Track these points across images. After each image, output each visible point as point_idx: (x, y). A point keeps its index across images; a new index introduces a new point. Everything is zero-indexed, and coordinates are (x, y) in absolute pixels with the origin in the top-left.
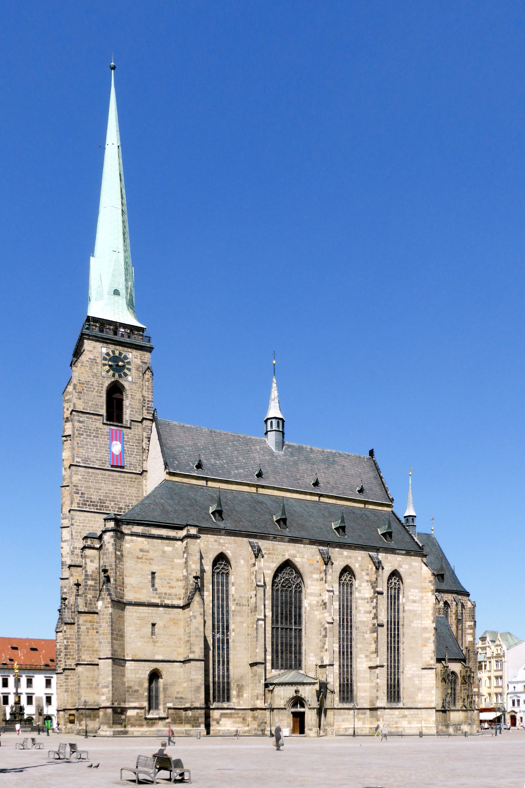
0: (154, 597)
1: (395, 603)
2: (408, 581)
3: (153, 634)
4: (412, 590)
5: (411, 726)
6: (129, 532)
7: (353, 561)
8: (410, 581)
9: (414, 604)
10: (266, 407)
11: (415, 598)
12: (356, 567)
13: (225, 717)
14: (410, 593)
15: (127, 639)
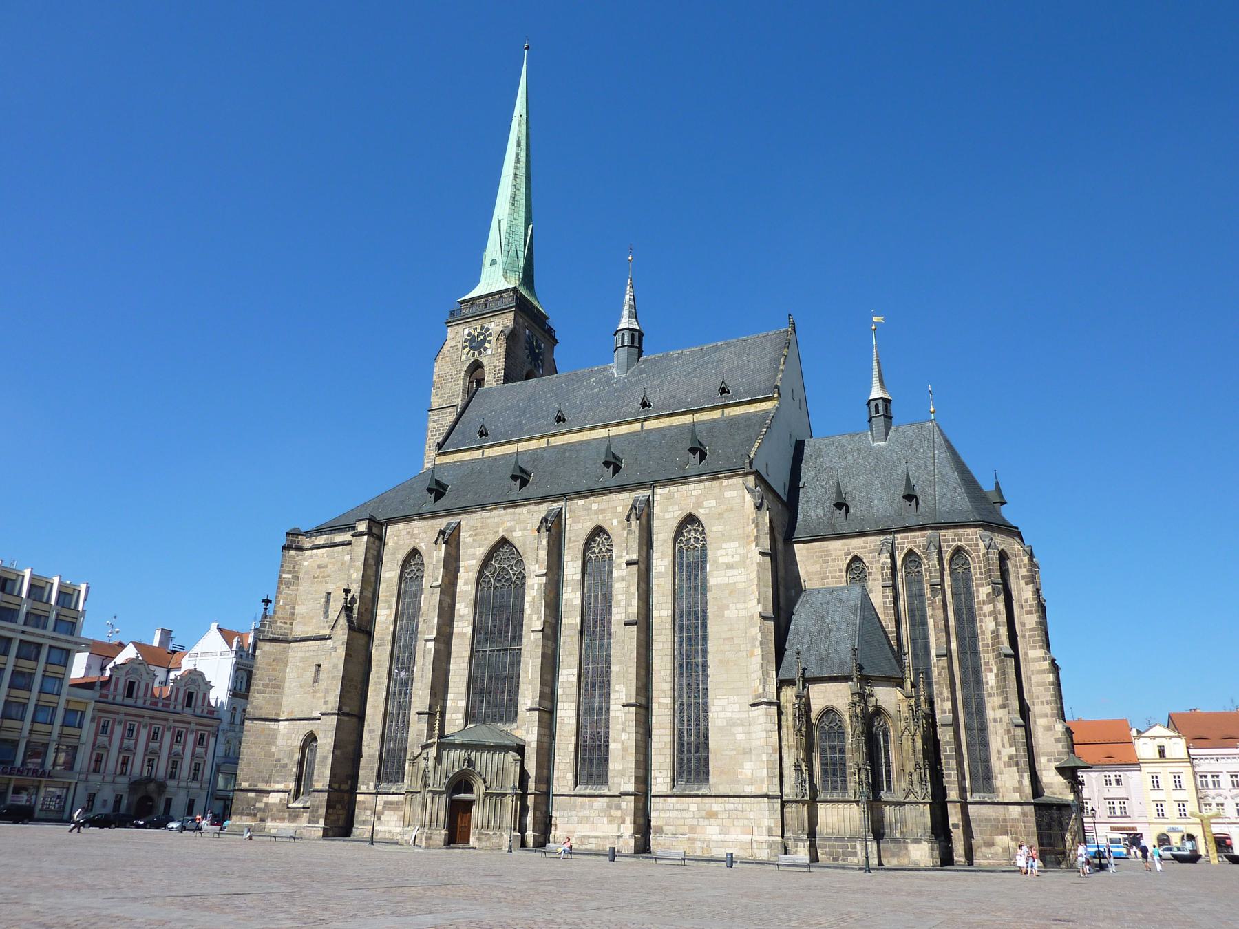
0: (324, 628)
1: (696, 576)
2: (714, 529)
3: (316, 680)
4: (724, 546)
5: (728, 838)
6: (309, 545)
7: (608, 516)
8: (720, 528)
9: (730, 572)
10: (619, 319)
11: (731, 560)
12: (614, 524)
13: (390, 809)
14: (720, 552)
15: (287, 691)
